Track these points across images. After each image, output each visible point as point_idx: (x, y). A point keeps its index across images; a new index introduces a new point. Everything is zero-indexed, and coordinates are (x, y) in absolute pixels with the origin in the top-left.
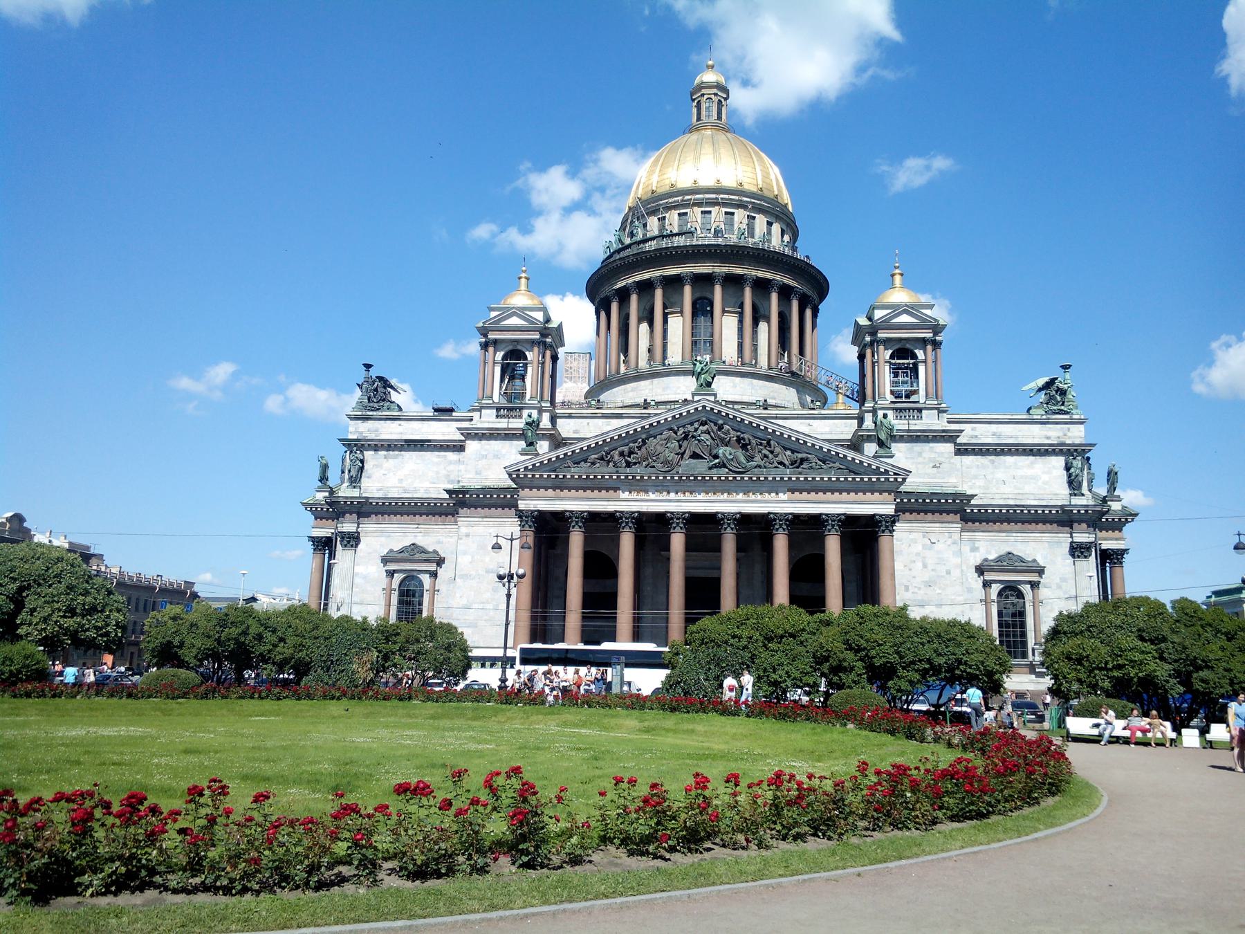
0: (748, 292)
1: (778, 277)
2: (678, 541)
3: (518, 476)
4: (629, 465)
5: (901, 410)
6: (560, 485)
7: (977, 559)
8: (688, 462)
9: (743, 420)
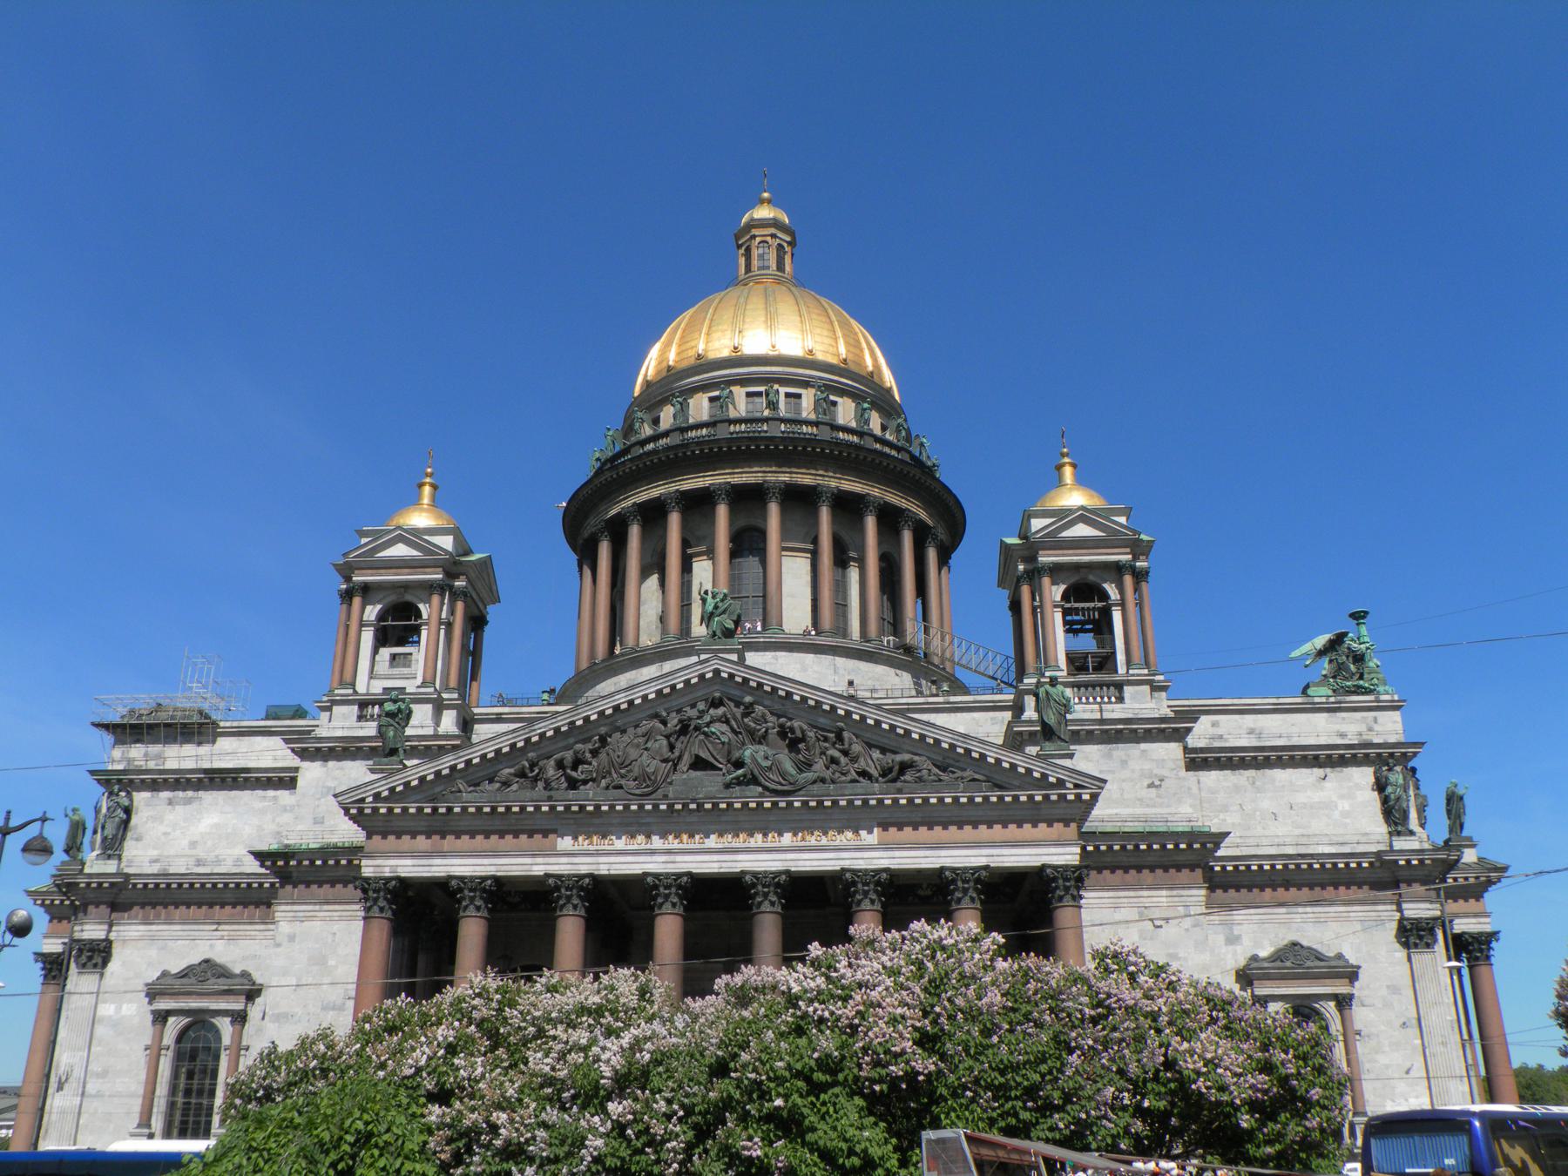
0: (825, 514)
1: (875, 492)
3: (361, 810)
4: (573, 784)
5: (1086, 685)
6: (441, 827)
7: (1237, 957)
8: (685, 775)
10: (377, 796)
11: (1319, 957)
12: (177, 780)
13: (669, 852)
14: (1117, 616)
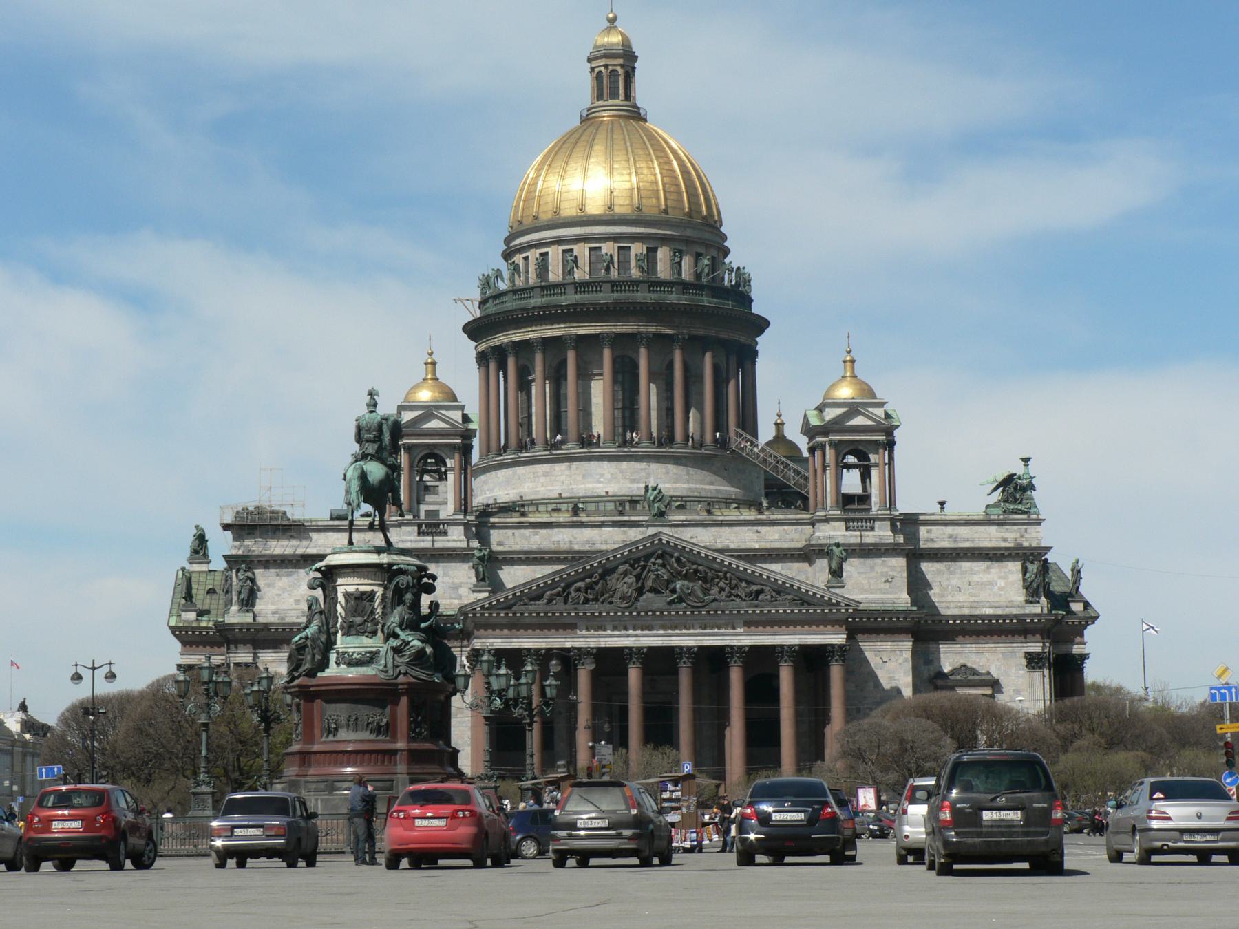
2: (634, 675)
3: (474, 615)
4: (586, 601)
9: (699, 553)
10: (482, 607)
11: (974, 672)
12: (283, 561)
13: (636, 636)
14: (875, 473)
